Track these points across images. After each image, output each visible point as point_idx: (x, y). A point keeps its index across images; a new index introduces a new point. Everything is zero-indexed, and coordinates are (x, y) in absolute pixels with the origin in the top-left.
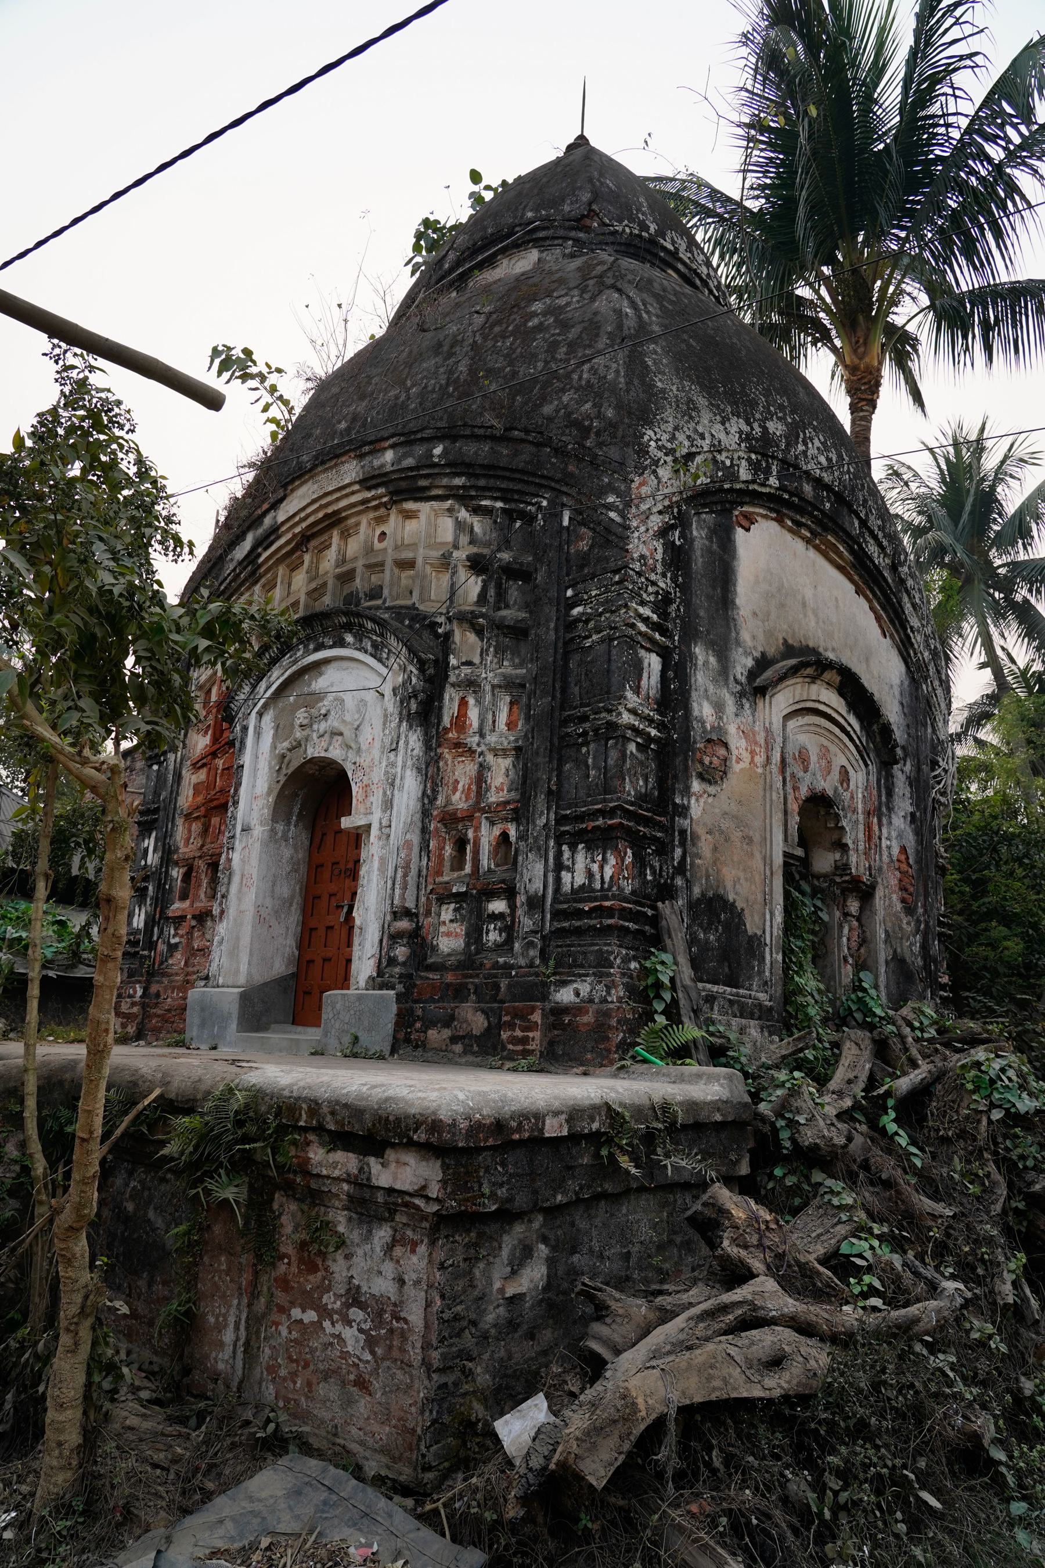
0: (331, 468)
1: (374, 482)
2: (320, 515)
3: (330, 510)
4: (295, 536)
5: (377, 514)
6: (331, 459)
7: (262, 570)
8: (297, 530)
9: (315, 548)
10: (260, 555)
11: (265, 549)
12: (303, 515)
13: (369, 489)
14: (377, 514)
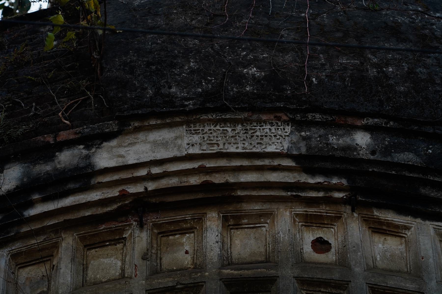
0: (242, 122)
1: (328, 165)
2: (194, 180)
3: (218, 179)
4: (124, 195)
5: (311, 210)
6: (242, 110)
7: (25, 229)
8: (132, 189)
9: (156, 225)
10: (31, 204)
11: (45, 200)
12: (156, 170)
13: (312, 172)
14: (311, 210)
